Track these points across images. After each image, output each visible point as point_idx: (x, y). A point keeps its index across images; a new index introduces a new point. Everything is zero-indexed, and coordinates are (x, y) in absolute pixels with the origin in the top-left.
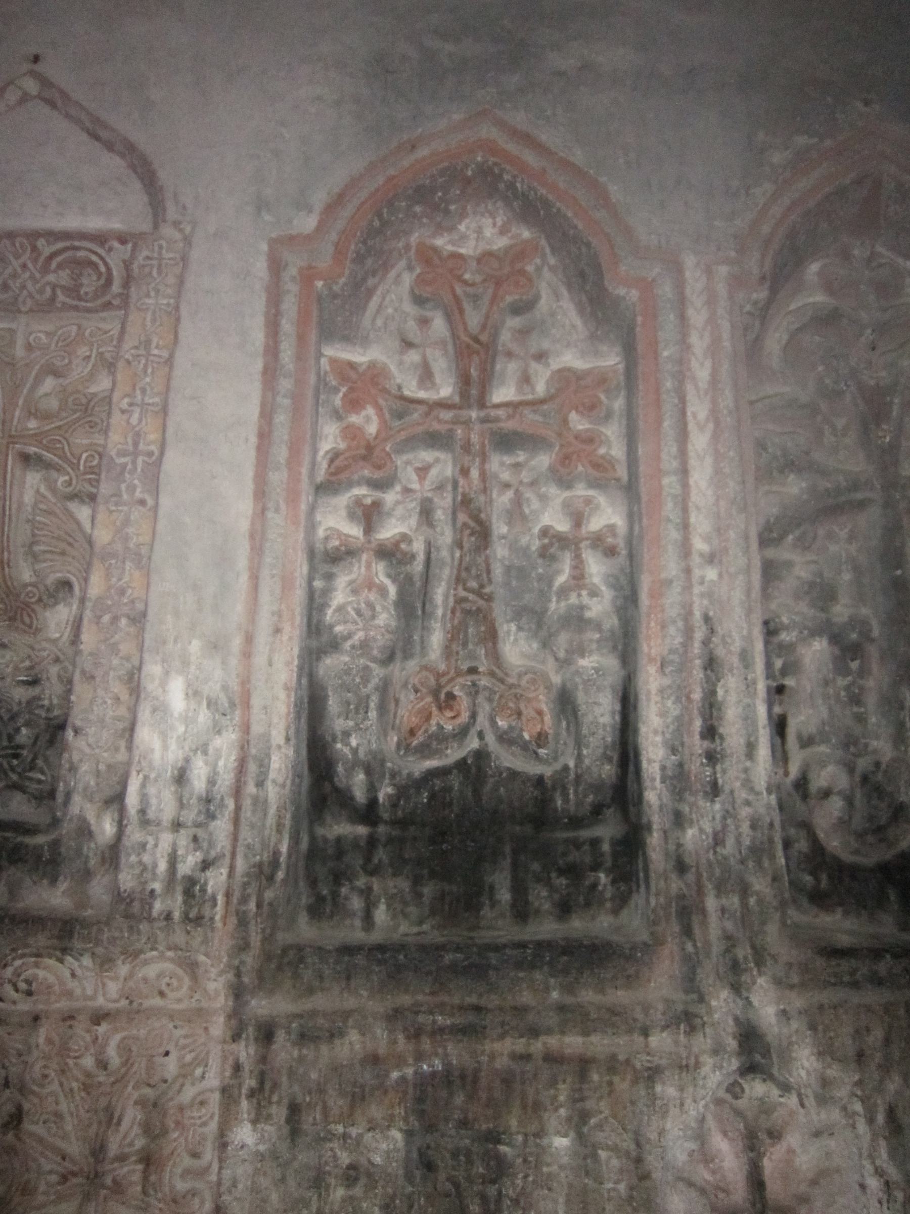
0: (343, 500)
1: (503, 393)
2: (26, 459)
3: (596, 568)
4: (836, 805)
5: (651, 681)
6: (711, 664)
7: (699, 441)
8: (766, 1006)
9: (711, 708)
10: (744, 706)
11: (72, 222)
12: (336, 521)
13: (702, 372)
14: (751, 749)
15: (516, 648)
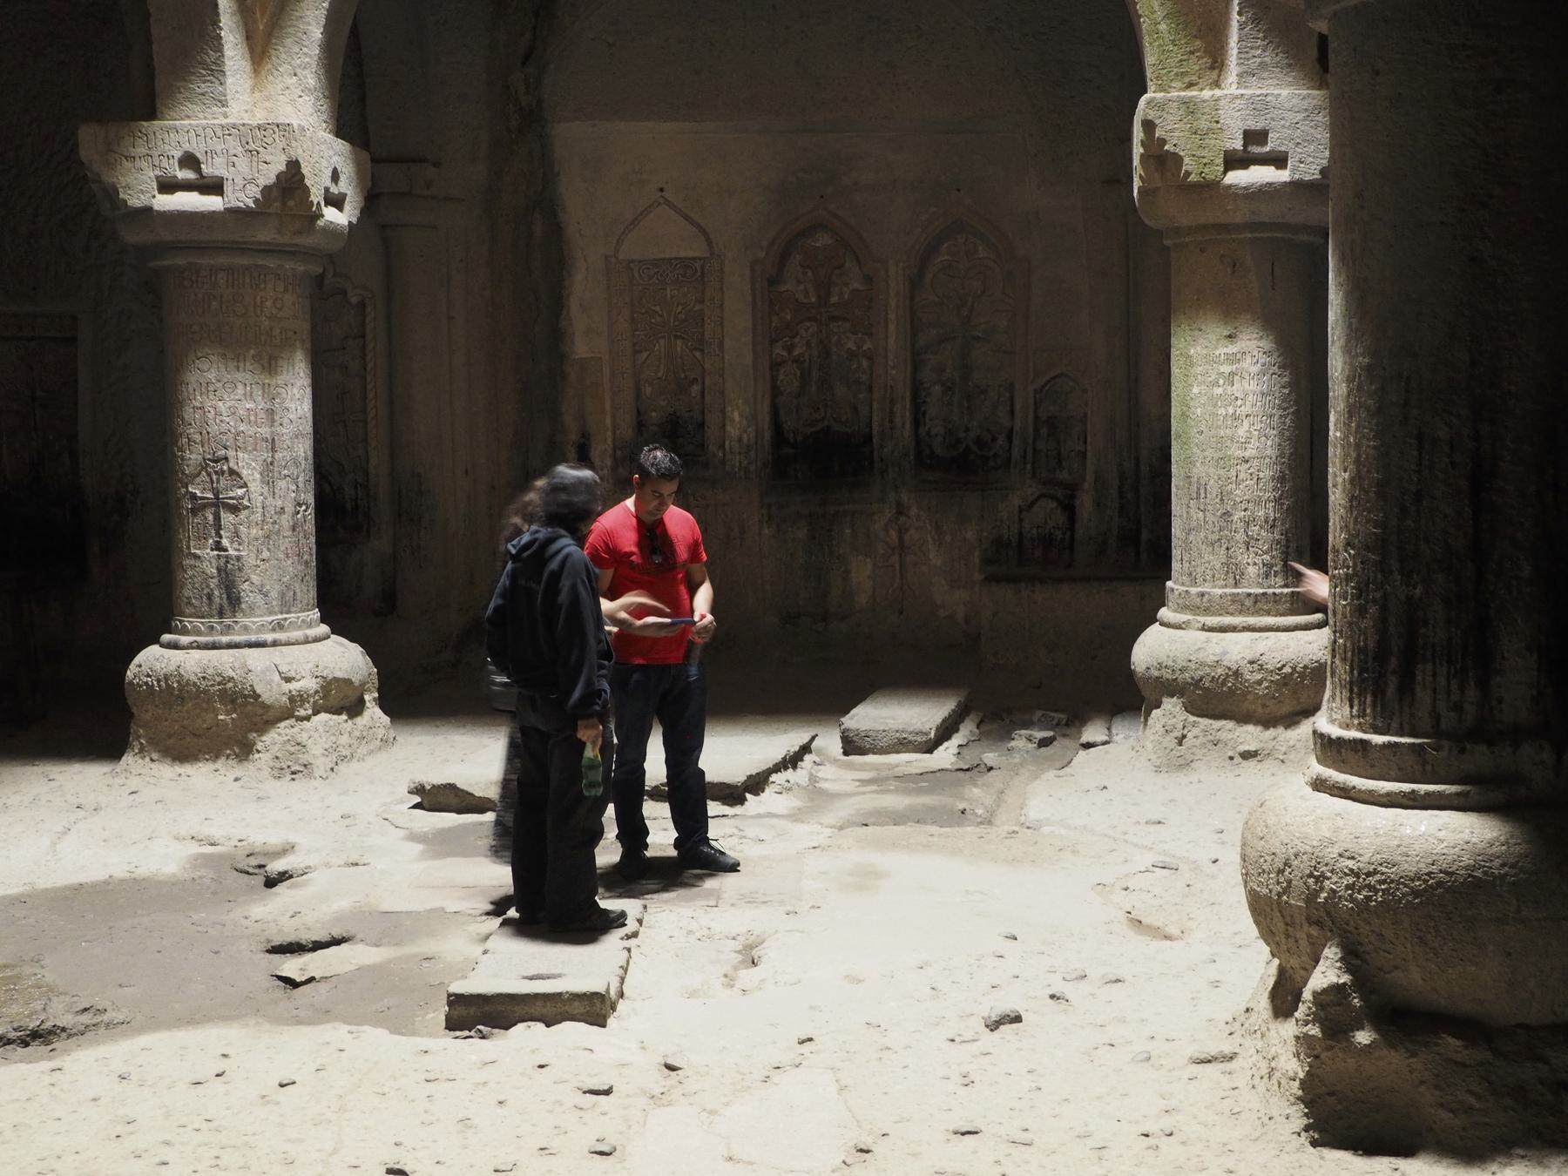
0: (780, 344)
1: (834, 299)
2: (676, 337)
3: (865, 363)
4: (940, 439)
5: (875, 406)
6: (893, 402)
7: (892, 327)
8: (905, 497)
9: (892, 413)
10: (904, 414)
11: (683, 254)
12: (779, 350)
13: (893, 303)
14: (903, 426)
15: (840, 390)
